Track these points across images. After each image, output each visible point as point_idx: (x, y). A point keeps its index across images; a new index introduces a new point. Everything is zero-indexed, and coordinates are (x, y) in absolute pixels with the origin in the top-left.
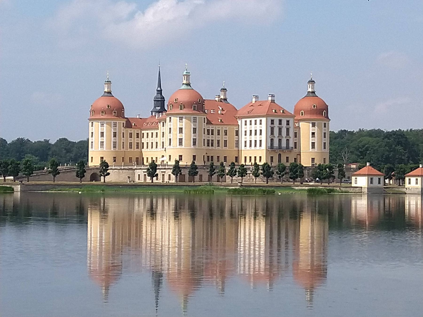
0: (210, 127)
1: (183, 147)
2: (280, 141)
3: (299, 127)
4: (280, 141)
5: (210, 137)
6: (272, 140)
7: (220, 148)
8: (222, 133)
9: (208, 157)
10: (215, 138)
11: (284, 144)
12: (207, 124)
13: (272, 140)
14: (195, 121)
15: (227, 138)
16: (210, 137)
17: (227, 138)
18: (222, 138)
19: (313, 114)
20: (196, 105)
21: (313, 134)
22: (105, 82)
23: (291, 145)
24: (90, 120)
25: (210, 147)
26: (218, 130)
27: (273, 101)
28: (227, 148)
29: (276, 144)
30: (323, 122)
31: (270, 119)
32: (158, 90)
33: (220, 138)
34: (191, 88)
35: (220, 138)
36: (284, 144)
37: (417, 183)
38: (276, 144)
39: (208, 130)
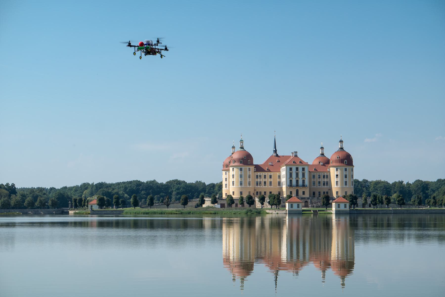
0: (259, 174)
1: (235, 186)
2: (297, 181)
3: (329, 172)
4: (297, 181)
5: (259, 180)
6: (291, 181)
7: (266, 186)
8: (268, 177)
9: (257, 192)
10: (263, 180)
11: (300, 183)
12: (254, 172)
13: (291, 181)
14: (241, 170)
15: (272, 180)
16: (259, 180)
17: (272, 180)
18: (268, 180)
19: (337, 162)
20: (242, 161)
21: (337, 175)
22: (232, 147)
23: (307, 183)
24: (223, 170)
25: (259, 186)
26: (264, 175)
27: (296, 156)
28: (272, 187)
29: (294, 183)
30: (344, 168)
31: (288, 167)
32: (274, 151)
33: (266, 180)
34: (243, 150)
35: (266, 180)
36: (300, 183)
37: (345, 207)
38: (294, 183)
39: (257, 176)
